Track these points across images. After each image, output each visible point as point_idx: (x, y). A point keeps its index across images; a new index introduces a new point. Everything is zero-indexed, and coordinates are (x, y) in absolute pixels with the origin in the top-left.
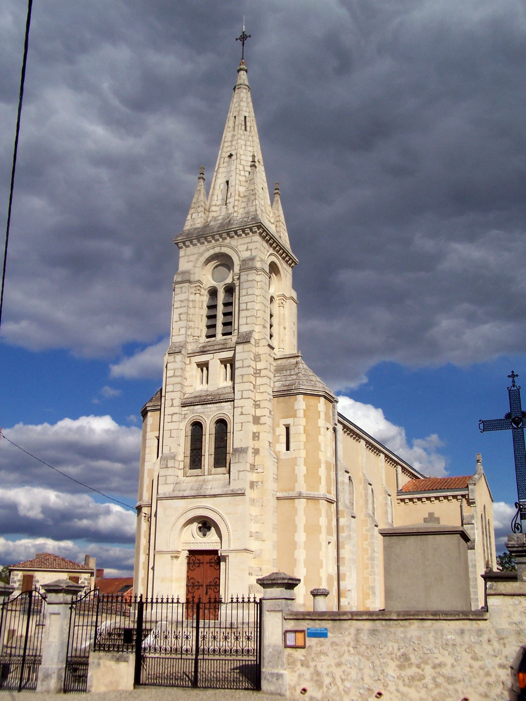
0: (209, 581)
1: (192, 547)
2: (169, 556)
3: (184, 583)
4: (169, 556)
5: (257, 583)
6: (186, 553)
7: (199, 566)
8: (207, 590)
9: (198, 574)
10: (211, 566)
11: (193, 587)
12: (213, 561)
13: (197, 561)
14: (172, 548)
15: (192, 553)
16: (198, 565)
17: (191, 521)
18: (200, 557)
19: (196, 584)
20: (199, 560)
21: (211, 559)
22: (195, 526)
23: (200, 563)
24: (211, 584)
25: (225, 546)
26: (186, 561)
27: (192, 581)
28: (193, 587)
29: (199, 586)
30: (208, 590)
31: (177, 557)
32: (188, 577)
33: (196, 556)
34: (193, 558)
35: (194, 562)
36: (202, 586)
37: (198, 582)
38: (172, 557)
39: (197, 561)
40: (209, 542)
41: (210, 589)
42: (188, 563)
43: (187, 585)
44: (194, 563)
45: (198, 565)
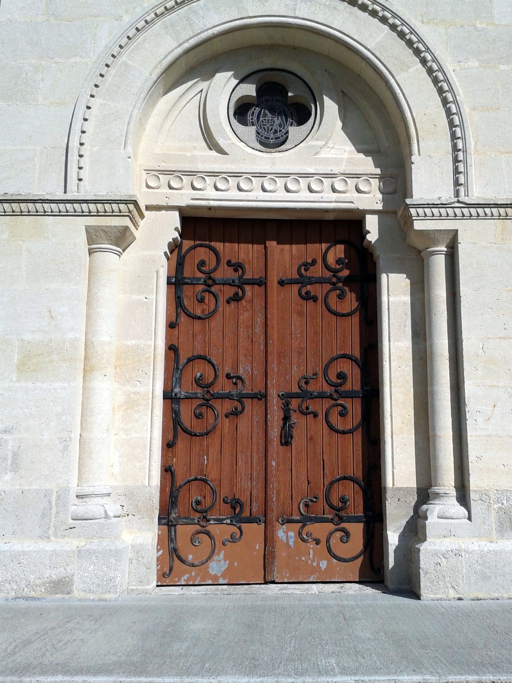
0: (297, 372)
1: (211, 193)
2: (73, 231)
3: (153, 383)
4: (73, 231)
5: (347, 542)
6: (170, 226)
7: (236, 298)
8: (286, 418)
9: (232, 339)
10: (307, 297)
11: (206, 403)
12: (318, 271)
13: (224, 273)
14: (93, 185)
15: (199, 226)
16: (230, 291)
17: (197, 63)
18: (247, 252)
19: (224, 386)
20: (238, 267)
21: (306, 266)
22: (224, 89)
23: (242, 284)
24: (311, 388)
25: (429, 180)
26: (162, 269)
27: (199, 370)
28: (206, 403)
29: (241, 398)
30: (295, 418)
31: (122, 239)
32: (172, 349)
33: (219, 246)
34: (202, 253)
35: (209, 275)
36: (262, 397)
37: (235, 378)
38: (93, 236)
39: (224, 273)
40: (321, 167)
41: (305, 413)
42: (176, 282)
43: (169, 396)
44: (210, 282)
45: (230, 291)
